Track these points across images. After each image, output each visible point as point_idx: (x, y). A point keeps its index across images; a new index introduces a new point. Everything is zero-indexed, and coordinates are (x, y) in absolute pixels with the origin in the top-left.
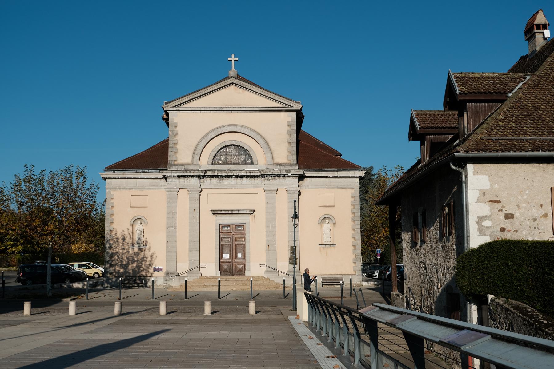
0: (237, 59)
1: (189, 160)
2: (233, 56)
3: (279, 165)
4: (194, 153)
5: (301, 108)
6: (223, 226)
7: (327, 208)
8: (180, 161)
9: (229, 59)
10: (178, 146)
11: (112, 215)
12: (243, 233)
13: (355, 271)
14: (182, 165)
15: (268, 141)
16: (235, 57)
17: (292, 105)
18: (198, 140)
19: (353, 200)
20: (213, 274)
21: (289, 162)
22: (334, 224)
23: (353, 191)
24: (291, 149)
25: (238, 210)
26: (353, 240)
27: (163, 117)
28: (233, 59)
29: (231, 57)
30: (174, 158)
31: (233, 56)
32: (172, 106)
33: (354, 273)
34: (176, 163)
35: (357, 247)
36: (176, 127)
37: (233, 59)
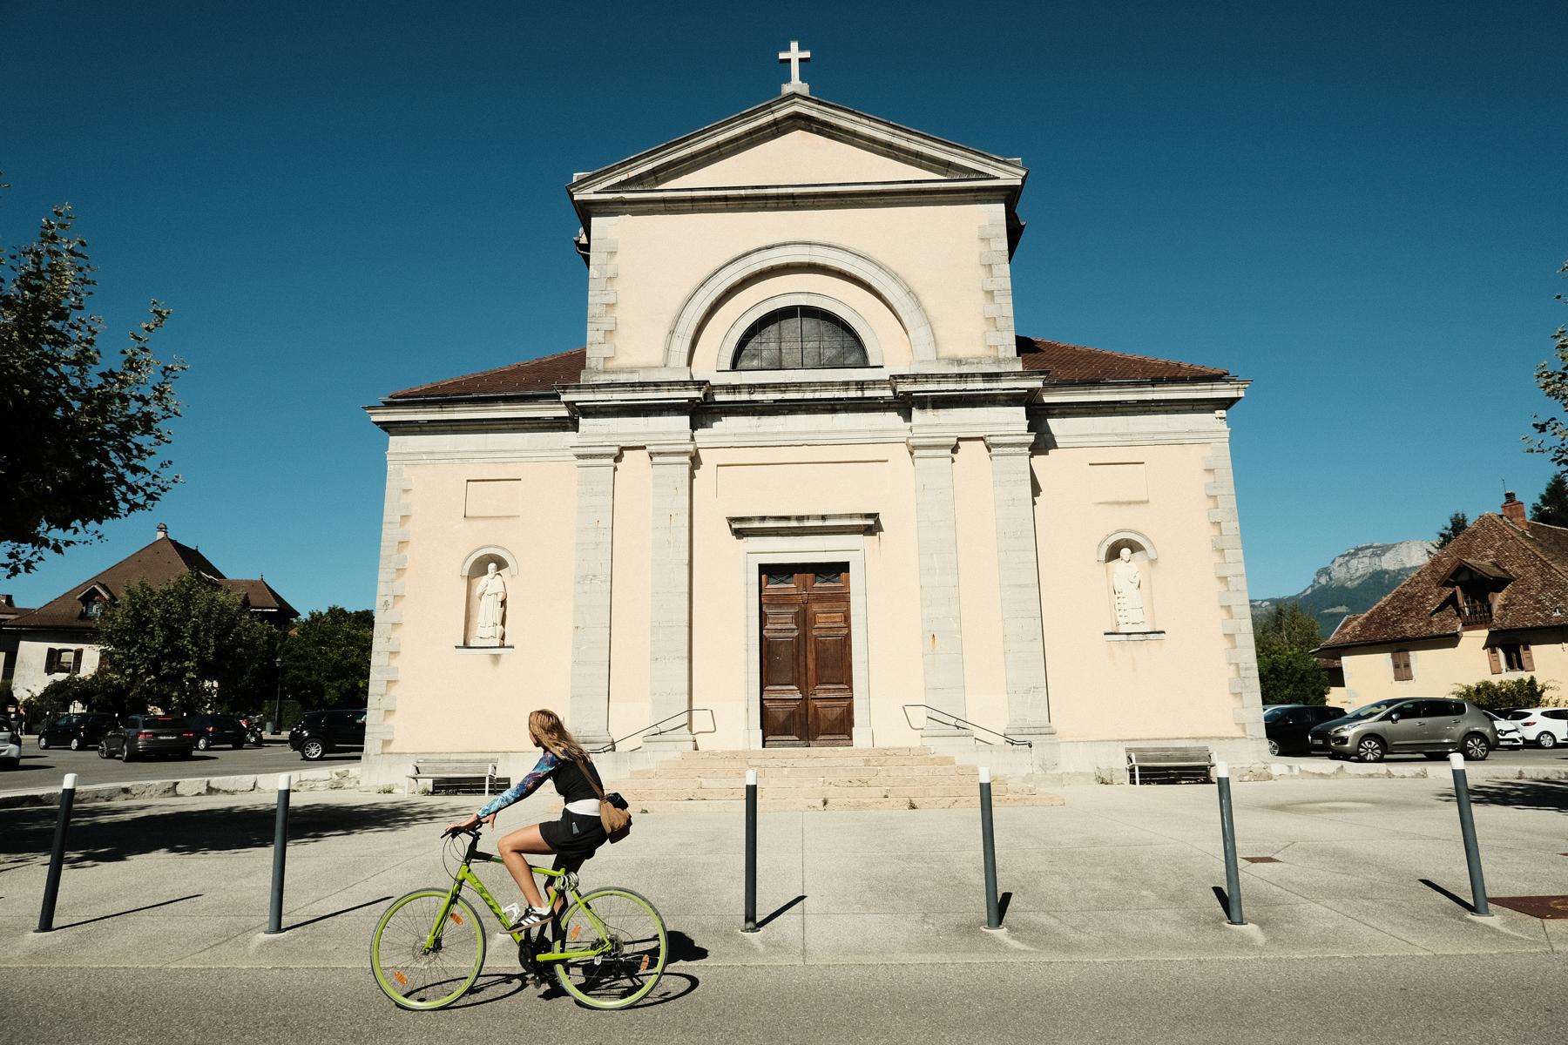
0: (807, 54)
1: (656, 357)
2: (794, 45)
3: (959, 362)
4: (672, 332)
5: (1024, 180)
6: (769, 572)
7: (1124, 507)
8: (622, 361)
9: (782, 56)
10: (618, 313)
11: (403, 543)
12: (843, 598)
13: (1243, 726)
14: (632, 371)
15: (917, 288)
16: (801, 49)
17: (991, 171)
18: (687, 291)
19: (1209, 478)
20: (739, 745)
21: (992, 352)
22: (1153, 562)
23: (1207, 451)
24: (993, 311)
25: (824, 518)
26: (1223, 614)
27: (577, 242)
28: (795, 54)
29: (788, 49)
30: (606, 351)
31: (794, 45)
32: (598, 187)
33: (1240, 734)
34: (610, 365)
35: (1239, 638)
36: (612, 253)
37: (795, 54)
